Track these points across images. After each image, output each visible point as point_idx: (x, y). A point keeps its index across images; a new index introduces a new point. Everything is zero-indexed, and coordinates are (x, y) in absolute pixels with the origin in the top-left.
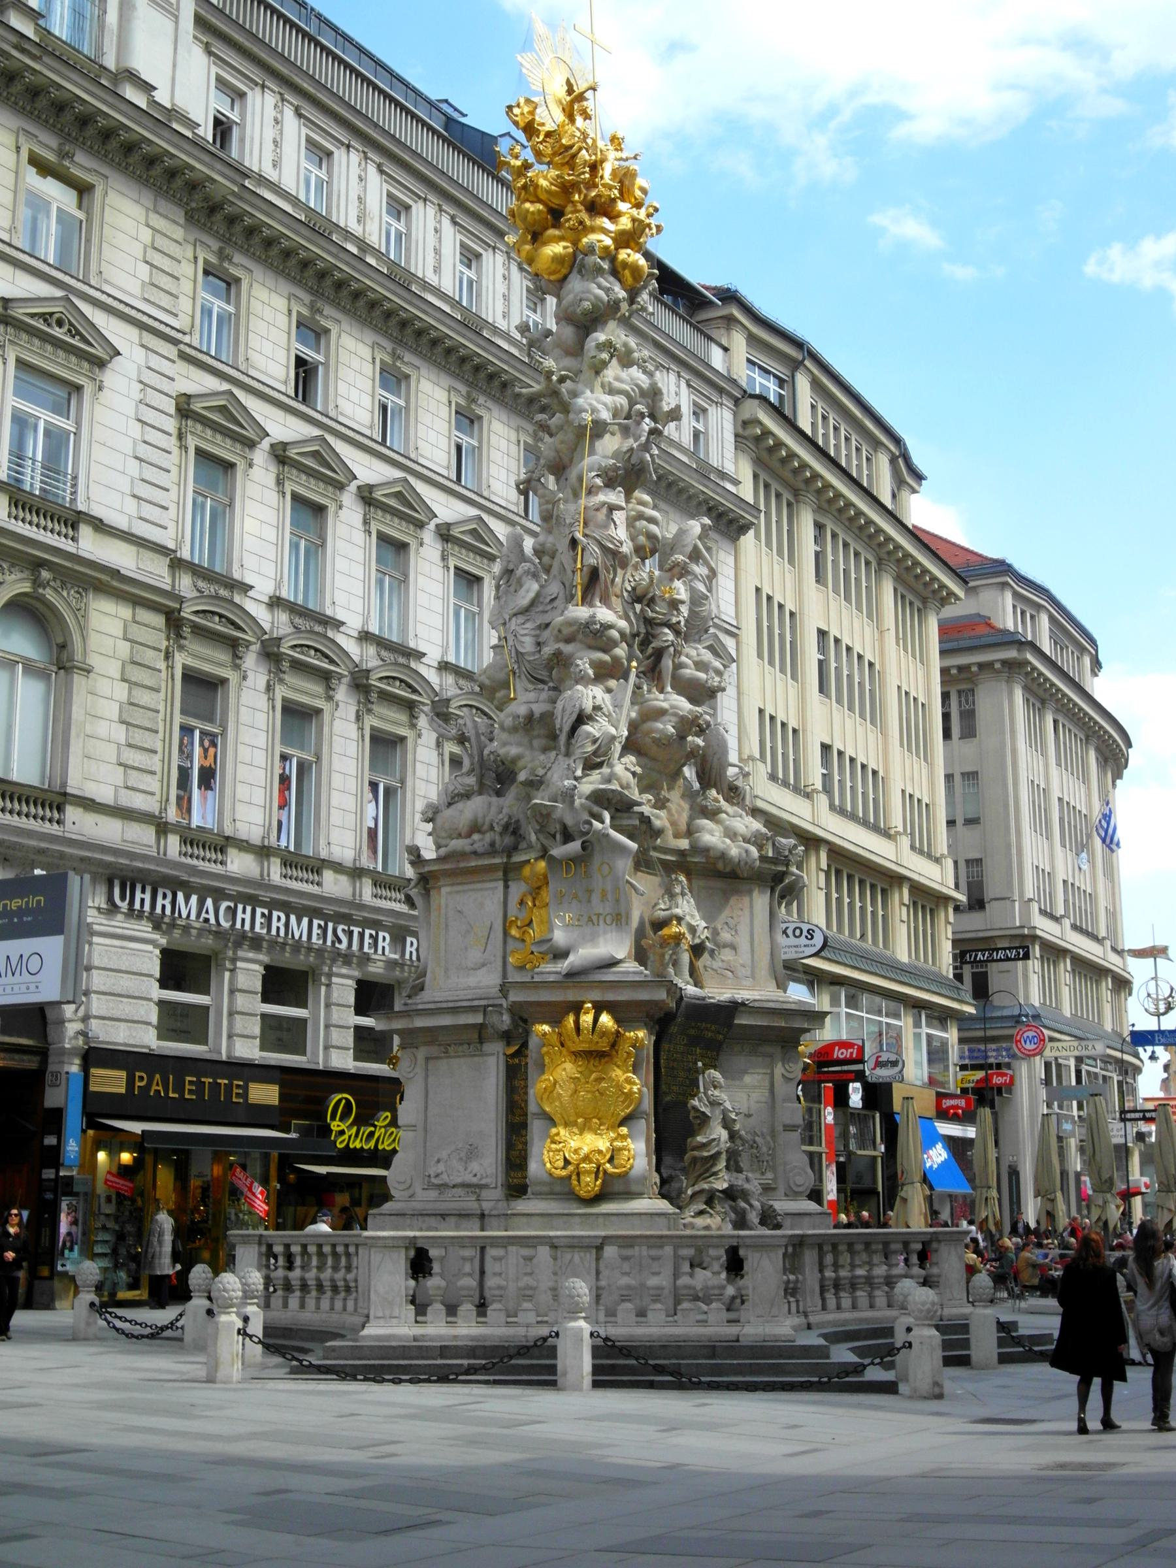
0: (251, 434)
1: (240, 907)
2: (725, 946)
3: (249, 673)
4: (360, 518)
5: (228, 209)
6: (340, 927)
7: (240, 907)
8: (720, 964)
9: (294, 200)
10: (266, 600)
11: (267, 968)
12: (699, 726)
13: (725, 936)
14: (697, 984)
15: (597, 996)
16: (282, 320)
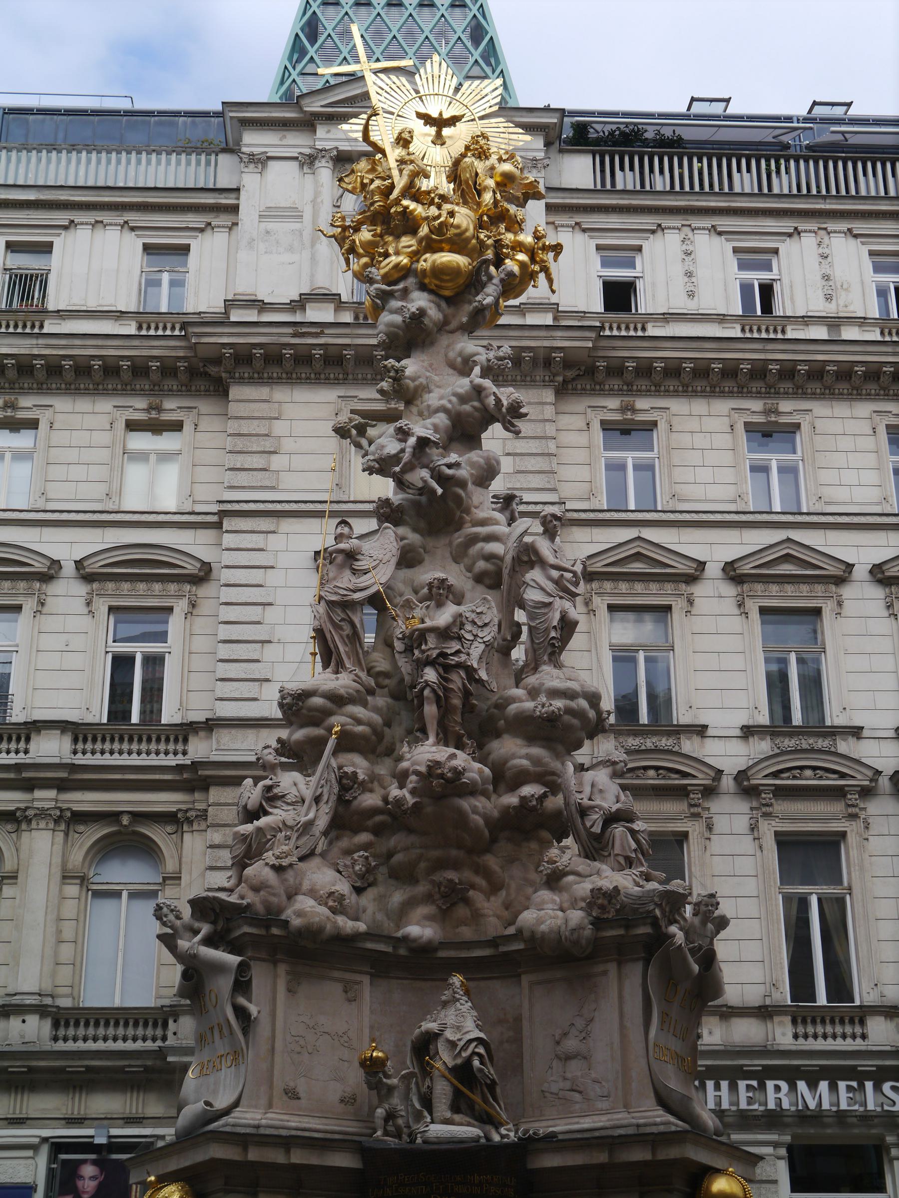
0: (682, 567)
1: (710, 1084)
2: (568, 1058)
3: (716, 819)
4: (882, 604)
5: (601, 364)
6: (887, 1087)
7: (710, 1084)
8: (562, 1085)
9: (721, 319)
10: (738, 733)
11: (790, 1148)
12: (442, 776)
13: (571, 1044)
14: (487, 1119)
15: (173, 1165)
16: (724, 440)
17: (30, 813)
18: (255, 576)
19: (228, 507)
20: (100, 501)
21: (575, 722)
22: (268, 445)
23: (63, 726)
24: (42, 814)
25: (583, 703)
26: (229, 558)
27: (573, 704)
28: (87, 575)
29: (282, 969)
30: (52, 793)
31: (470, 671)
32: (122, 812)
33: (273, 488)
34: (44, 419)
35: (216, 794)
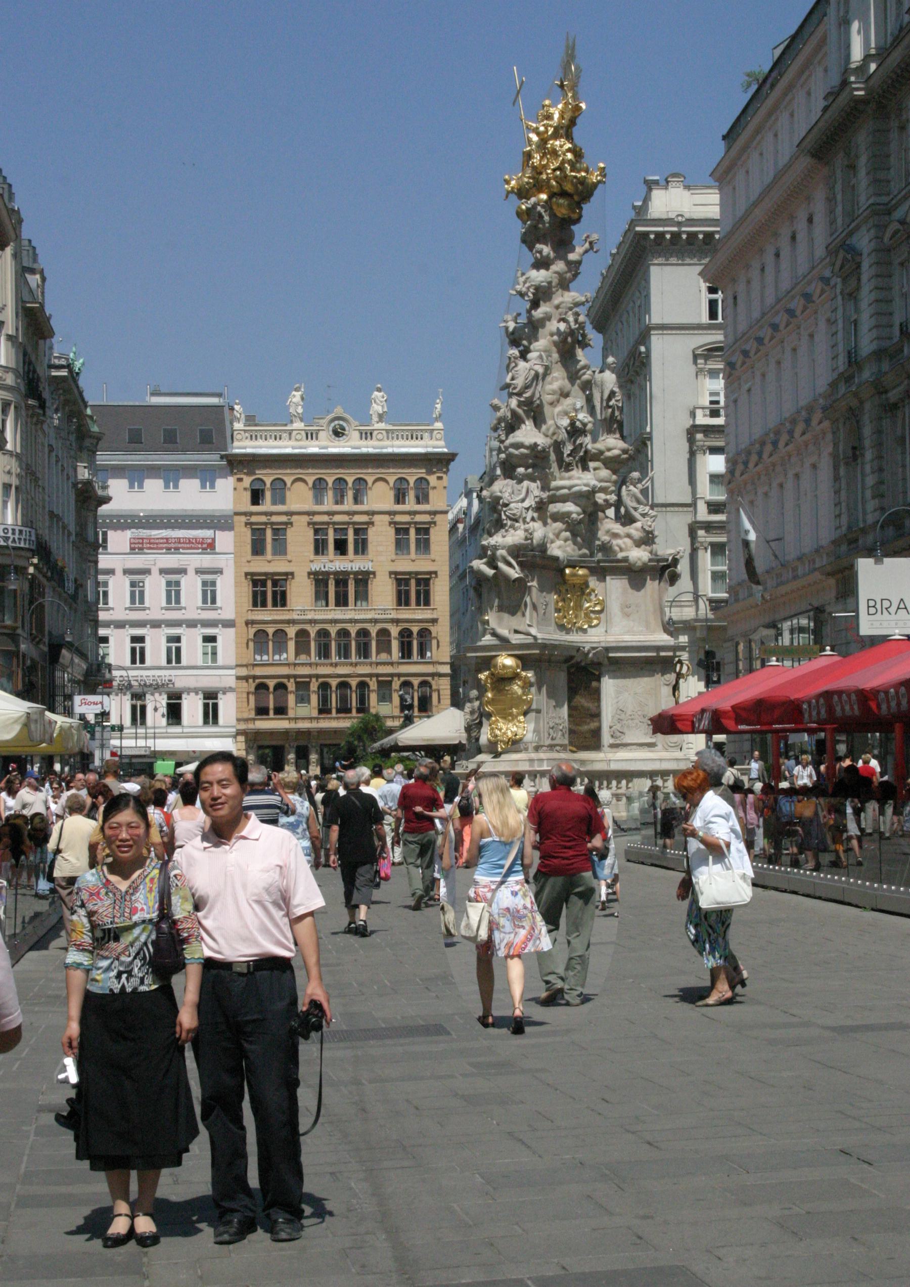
25: (511, 450)
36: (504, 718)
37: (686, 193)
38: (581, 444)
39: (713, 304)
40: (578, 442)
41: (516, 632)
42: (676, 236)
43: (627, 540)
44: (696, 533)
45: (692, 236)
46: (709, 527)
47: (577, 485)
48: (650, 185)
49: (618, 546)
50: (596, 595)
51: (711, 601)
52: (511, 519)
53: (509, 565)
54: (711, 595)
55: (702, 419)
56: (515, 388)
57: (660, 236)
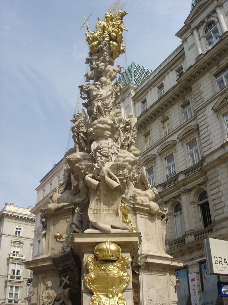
17: (180, 193)
18: (204, 122)
19: (196, 111)
20: (180, 124)
21: (99, 130)
22: (200, 93)
23: (182, 173)
24: (182, 193)
26: (199, 121)
27: (95, 127)
28: (181, 140)
29: (51, 221)
30: (183, 187)
31: (83, 132)
32: (196, 185)
33: (203, 101)
34: (168, 114)
35: (209, 173)
36: (107, 296)
37: (14, 207)
38: (129, 138)
39: (16, 232)
40: (128, 136)
41: (113, 227)
42: (11, 215)
43: (145, 197)
44: (7, 283)
45: (14, 216)
46: (10, 281)
47: (128, 157)
48: (6, 204)
49: (140, 200)
50: (131, 225)
51: (8, 300)
52: (104, 156)
53: (111, 177)
54: (9, 298)
55: (11, 256)
56: (100, 97)
57: (8, 215)
